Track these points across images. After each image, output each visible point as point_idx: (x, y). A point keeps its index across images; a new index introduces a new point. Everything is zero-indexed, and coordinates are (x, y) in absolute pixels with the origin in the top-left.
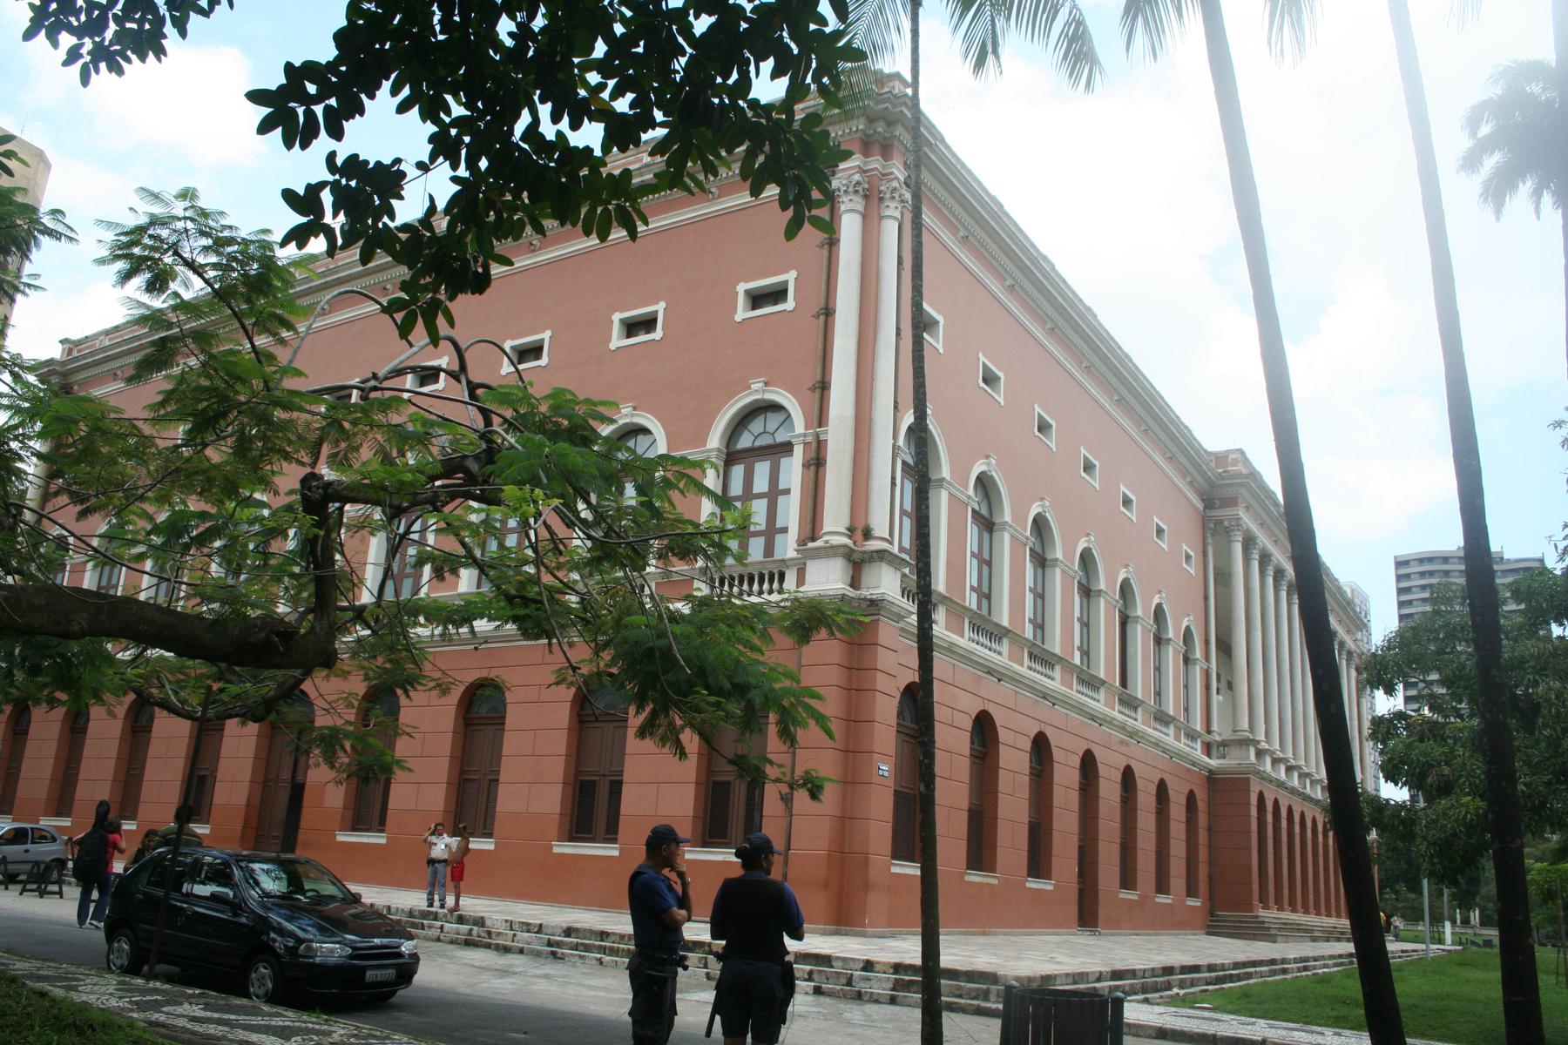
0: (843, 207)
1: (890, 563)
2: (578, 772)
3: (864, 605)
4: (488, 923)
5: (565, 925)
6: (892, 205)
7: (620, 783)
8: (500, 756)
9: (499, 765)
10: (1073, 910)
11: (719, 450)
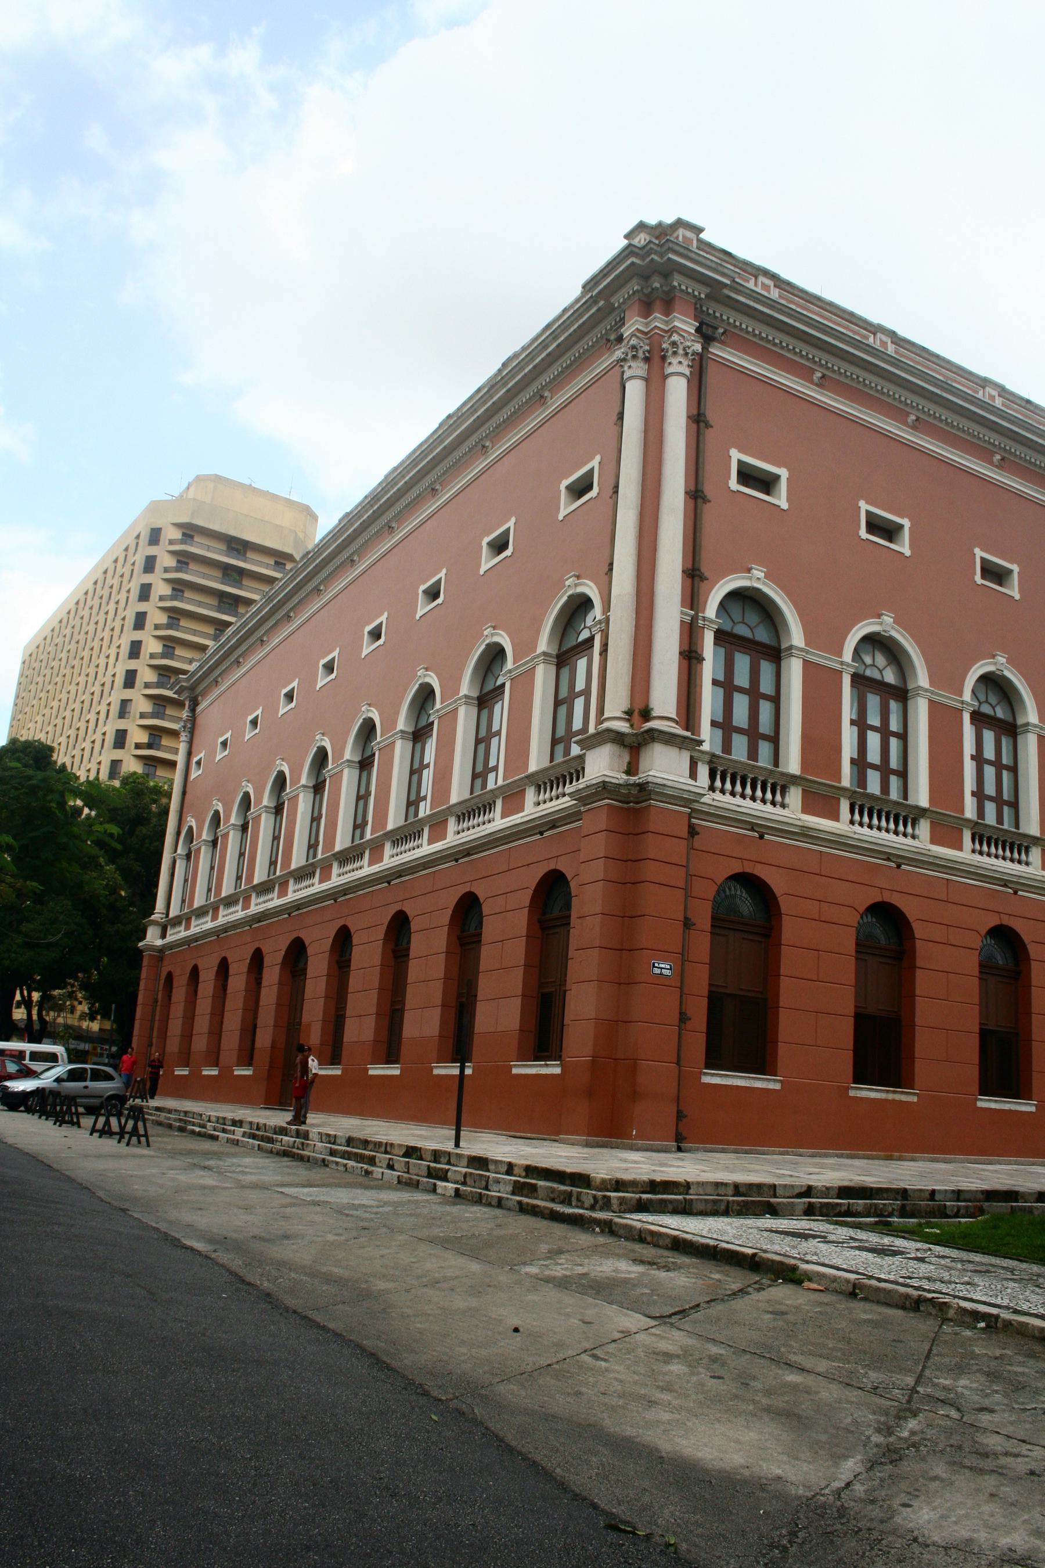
0: (625, 377)
3: (634, 791)
4: (311, 1136)
6: (674, 361)
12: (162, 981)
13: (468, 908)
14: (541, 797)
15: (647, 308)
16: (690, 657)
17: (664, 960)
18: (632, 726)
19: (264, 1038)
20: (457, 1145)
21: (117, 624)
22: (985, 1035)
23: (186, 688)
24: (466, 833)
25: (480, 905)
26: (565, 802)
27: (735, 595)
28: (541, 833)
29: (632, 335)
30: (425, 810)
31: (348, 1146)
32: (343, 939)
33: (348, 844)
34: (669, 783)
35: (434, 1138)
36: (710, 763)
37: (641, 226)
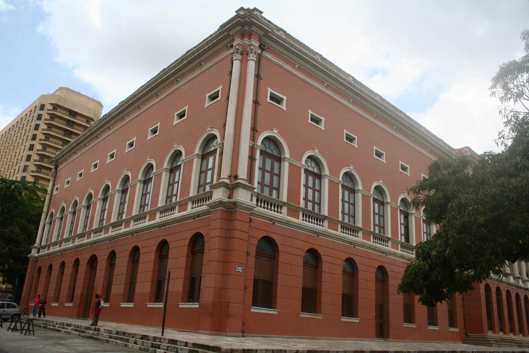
3: (231, 205)
4: (101, 330)
6: (251, 55)
10: (373, 331)
11: (197, 154)
12: (37, 270)
13: (163, 245)
14: (194, 206)
15: (242, 36)
16: (252, 158)
17: (240, 266)
18: (231, 181)
19: (78, 292)
20: (163, 335)
21: (25, 138)
22: (343, 295)
23: (54, 161)
24: (163, 218)
25: (168, 244)
26: (205, 208)
27: (267, 138)
28: (194, 219)
29: (237, 45)
30: (147, 209)
32: (113, 255)
33: (116, 220)
34: (244, 202)
35: (153, 332)
36: (257, 196)
37: (242, 9)
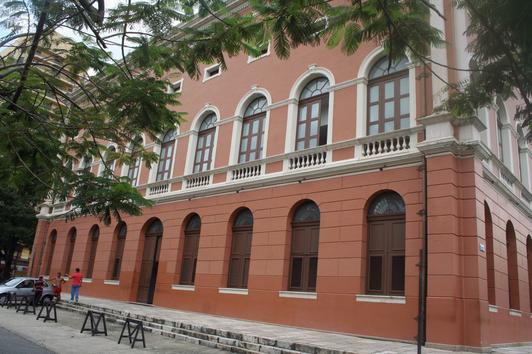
1: (476, 126)
2: (292, 254)
4: (245, 338)
5: (291, 342)
7: (316, 259)
8: (250, 246)
9: (250, 250)
11: (364, 78)
12: (49, 234)
31: (292, 349)
